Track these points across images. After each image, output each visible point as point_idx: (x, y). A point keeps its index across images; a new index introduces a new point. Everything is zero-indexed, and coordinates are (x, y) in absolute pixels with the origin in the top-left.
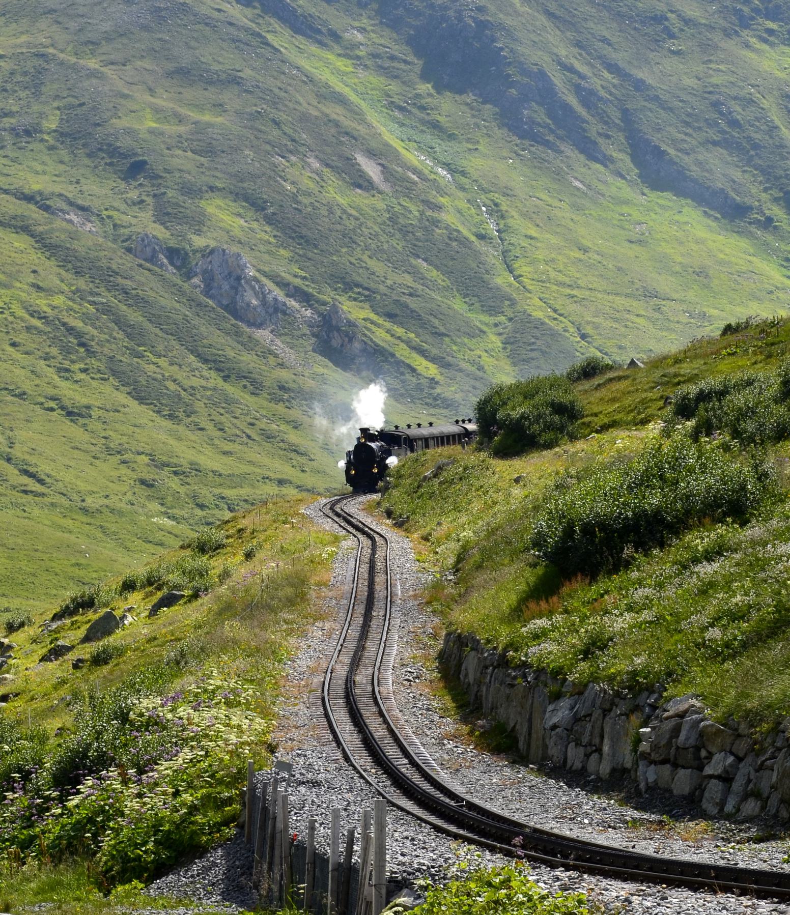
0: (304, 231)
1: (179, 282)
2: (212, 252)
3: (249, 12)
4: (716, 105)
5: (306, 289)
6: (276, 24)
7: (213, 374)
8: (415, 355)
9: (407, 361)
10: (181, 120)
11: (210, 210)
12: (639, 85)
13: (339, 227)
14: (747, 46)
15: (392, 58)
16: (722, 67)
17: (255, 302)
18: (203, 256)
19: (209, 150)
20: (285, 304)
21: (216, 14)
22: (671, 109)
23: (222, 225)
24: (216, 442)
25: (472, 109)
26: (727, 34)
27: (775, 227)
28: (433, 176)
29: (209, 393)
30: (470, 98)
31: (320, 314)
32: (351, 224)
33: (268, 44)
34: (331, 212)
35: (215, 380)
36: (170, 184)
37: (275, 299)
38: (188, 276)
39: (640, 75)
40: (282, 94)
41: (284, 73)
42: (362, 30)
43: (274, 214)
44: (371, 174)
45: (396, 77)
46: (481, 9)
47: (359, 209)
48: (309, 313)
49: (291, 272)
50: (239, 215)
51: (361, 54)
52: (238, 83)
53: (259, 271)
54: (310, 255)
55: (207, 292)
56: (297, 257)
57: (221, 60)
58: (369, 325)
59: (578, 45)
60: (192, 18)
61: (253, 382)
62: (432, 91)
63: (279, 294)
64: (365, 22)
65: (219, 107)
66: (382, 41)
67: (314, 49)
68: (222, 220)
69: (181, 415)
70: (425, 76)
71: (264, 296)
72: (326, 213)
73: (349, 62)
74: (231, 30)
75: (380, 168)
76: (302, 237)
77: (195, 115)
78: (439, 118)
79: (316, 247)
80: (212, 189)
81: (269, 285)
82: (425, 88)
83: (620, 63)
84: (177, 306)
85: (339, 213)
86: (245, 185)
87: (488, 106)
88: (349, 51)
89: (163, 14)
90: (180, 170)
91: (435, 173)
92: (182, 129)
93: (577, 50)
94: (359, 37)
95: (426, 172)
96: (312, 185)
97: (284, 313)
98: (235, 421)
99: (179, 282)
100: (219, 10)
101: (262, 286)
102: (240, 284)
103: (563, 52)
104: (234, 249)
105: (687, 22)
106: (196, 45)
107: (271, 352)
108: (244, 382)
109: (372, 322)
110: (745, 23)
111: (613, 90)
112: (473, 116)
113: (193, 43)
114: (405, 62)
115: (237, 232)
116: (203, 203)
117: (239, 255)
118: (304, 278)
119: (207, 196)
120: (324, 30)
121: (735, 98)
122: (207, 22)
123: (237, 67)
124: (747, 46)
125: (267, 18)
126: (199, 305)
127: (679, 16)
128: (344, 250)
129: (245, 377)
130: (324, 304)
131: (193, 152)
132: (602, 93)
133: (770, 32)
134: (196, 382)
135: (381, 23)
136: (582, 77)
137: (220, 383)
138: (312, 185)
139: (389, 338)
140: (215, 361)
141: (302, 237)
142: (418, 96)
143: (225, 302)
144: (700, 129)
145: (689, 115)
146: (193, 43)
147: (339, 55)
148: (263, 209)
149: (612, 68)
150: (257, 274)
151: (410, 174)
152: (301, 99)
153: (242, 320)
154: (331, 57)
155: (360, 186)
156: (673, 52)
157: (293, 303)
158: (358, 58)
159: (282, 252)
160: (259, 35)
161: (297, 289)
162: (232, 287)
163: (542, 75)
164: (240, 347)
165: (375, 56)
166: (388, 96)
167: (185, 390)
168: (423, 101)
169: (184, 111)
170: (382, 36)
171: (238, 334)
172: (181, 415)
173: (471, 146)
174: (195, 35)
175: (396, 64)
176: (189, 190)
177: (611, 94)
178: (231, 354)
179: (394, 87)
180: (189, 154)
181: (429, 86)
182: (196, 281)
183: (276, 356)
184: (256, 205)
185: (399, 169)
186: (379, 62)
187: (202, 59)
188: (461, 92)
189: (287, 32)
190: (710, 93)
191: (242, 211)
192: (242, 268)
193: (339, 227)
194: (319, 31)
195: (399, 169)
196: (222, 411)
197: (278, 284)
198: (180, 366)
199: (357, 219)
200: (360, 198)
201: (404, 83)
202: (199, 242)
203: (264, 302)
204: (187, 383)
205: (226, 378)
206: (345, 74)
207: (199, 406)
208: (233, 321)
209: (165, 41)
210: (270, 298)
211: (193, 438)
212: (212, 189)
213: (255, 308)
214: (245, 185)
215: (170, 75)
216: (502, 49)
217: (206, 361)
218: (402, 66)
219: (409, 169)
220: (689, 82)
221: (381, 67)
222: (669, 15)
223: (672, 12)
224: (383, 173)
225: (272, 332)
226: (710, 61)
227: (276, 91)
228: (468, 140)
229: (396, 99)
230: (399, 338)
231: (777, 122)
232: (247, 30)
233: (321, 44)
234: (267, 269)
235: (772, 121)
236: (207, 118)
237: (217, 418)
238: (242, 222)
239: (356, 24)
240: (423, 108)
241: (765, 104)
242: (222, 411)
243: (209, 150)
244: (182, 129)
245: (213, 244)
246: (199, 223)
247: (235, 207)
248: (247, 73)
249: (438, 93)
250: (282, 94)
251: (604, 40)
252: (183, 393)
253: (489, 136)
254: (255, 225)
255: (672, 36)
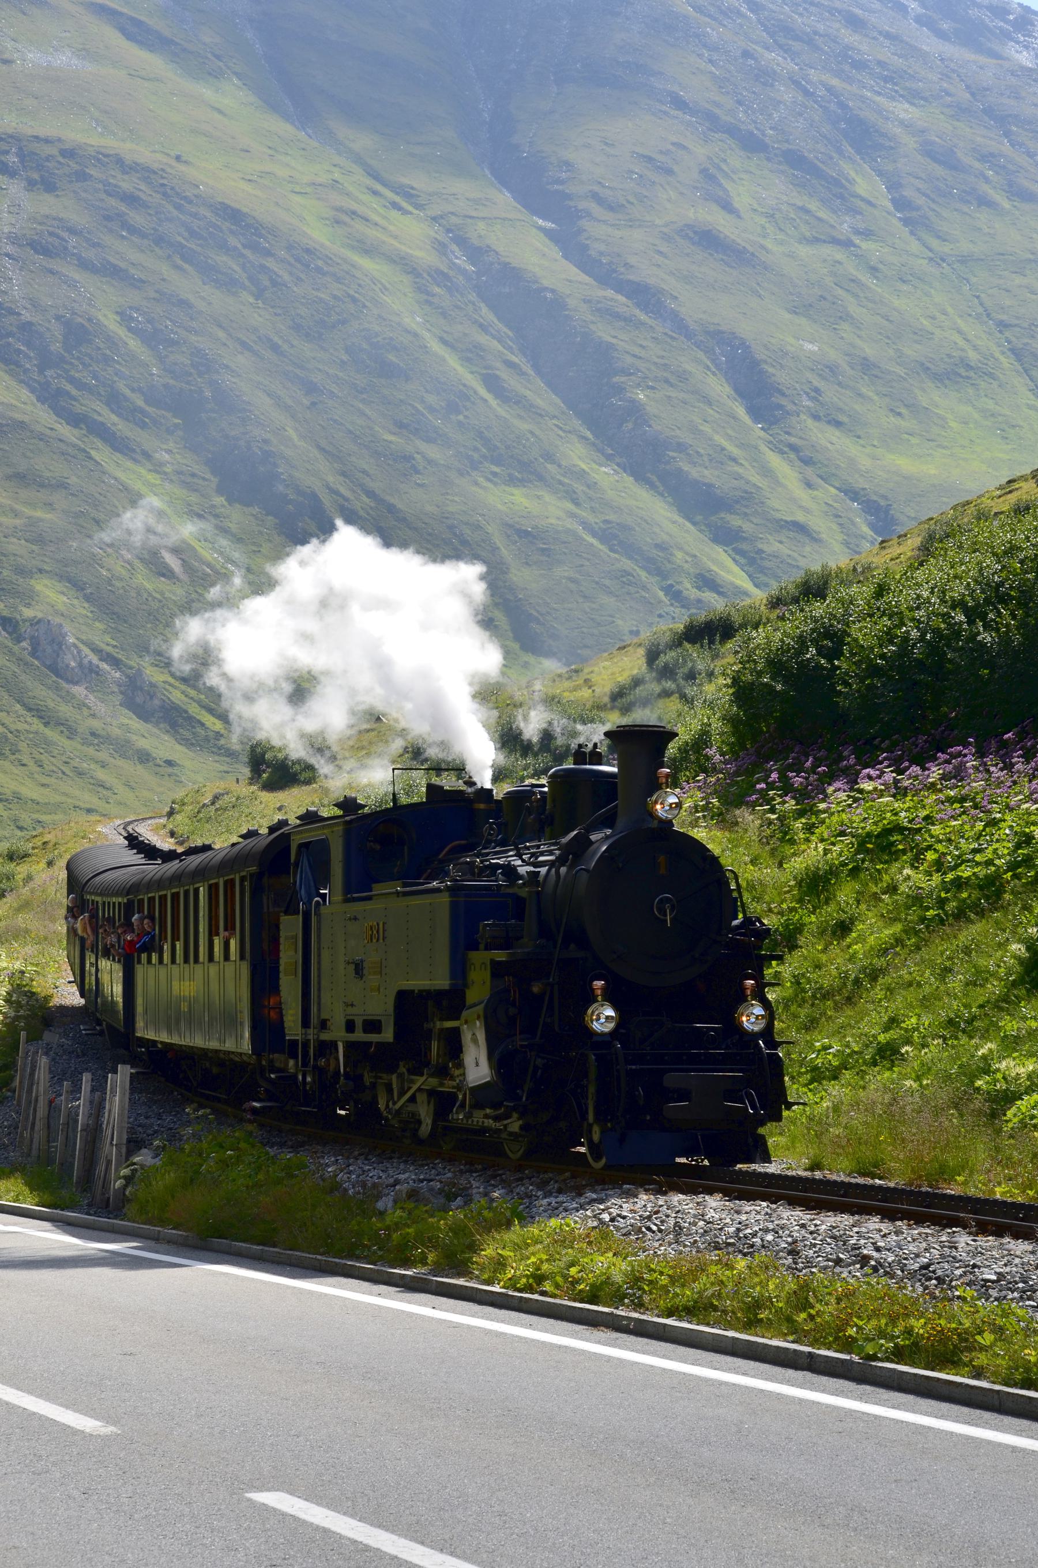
0: (116, 609)
1: (10, 644)
2: (39, 621)
3: (76, 431)
4: (451, 527)
5: (115, 655)
6: (99, 444)
7: (35, 720)
8: (204, 712)
9: (198, 717)
10: (16, 514)
11: (39, 587)
12: (391, 509)
13: (145, 607)
14: (476, 483)
15: (193, 475)
16: (456, 499)
17: (73, 664)
18: (31, 625)
19: (39, 540)
20: (98, 667)
21: (48, 432)
22: (416, 529)
23: (48, 600)
24: (36, 776)
25: (257, 519)
26: (461, 473)
27: (496, 626)
28: (224, 571)
29: (31, 736)
30: (256, 510)
31: (127, 676)
32: (155, 605)
33: (91, 458)
34: (139, 594)
35: (37, 725)
36: (5, 565)
37: (90, 662)
38: (19, 640)
39: (392, 501)
40: (102, 498)
41: (104, 482)
42: (169, 451)
43: (91, 594)
44: (173, 566)
45: (196, 490)
46: (265, 441)
47: (162, 594)
48: (118, 675)
49: (105, 641)
50: (63, 593)
51: (167, 470)
52: (66, 488)
53: (77, 639)
54: (121, 628)
55: (33, 654)
56: (110, 629)
57: (51, 468)
58: (167, 687)
59: (344, 474)
60: (29, 434)
61: (70, 728)
62: (225, 503)
63: (95, 660)
64: (171, 445)
65: (49, 506)
66: (185, 461)
67: (129, 464)
68: (48, 596)
69: (7, 753)
70: (220, 491)
71: (81, 659)
72: (135, 595)
73: (158, 476)
74: (61, 445)
75: (180, 562)
76: (114, 614)
77: (27, 511)
78: (230, 525)
79: (125, 622)
80: (41, 571)
81: (86, 650)
82: (220, 500)
83: (377, 492)
84: (8, 664)
85: (145, 595)
86: (69, 569)
87: (270, 518)
88: (157, 468)
89: (5, 429)
90: (15, 555)
91: (226, 568)
92: (18, 522)
93: (341, 478)
94: (167, 457)
95: (218, 567)
96: (124, 572)
97: (97, 674)
98: (52, 759)
99: (10, 644)
100: (52, 429)
101: (79, 652)
102: (60, 648)
103: (330, 479)
104: (58, 620)
105: (430, 462)
106: (32, 455)
107: (85, 705)
108: (62, 728)
109: (170, 685)
110: (474, 466)
111: (371, 512)
112: (258, 525)
113: (29, 454)
114: (204, 479)
115: (61, 607)
116: (33, 582)
117: (61, 625)
118: (115, 647)
119: (36, 576)
120: (138, 450)
121: (467, 524)
122: (41, 437)
123: (65, 475)
124: (476, 483)
125: (91, 437)
126: (26, 664)
127: (424, 457)
128: (149, 626)
129: (62, 724)
130: (131, 668)
131: (26, 540)
132: (362, 513)
133: (495, 474)
134: (21, 726)
135: (185, 447)
136: (347, 500)
137: (41, 727)
138: (124, 572)
139: (183, 697)
140: (38, 710)
141: (114, 614)
142: (213, 506)
143: (48, 663)
144: (438, 545)
145: (430, 534)
146: (29, 454)
147: (150, 470)
148: (83, 589)
149: (370, 494)
150: (76, 642)
151: (205, 568)
152: (117, 503)
153: (61, 678)
154: (143, 472)
155: (163, 575)
156: (419, 485)
157: (105, 666)
158: (165, 473)
159: (97, 624)
160: (84, 451)
161: (109, 655)
162: (54, 651)
163: (314, 496)
164: (59, 700)
165: (180, 473)
166: (190, 505)
167: (11, 733)
168: (217, 511)
169: (18, 507)
170: (186, 458)
171: (58, 689)
172: (7, 753)
173: (256, 549)
174: (31, 447)
175: (195, 480)
176: (21, 571)
177: (368, 514)
178: (51, 704)
179: (194, 498)
180: (23, 542)
181: (223, 499)
182: (24, 644)
183: (89, 708)
184: (77, 585)
185: (196, 564)
186: (183, 478)
187: (36, 467)
188: (248, 505)
189: (107, 450)
190: (447, 518)
191: (65, 590)
192: (64, 636)
193: (145, 607)
194: (134, 451)
195: (196, 564)
196: (42, 751)
197: (93, 650)
198: (8, 712)
199: (160, 601)
200: (163, 584)
201: (202, 495)
202: (28, 613)
203: (81, 665)
204: (13, 727)
205: (46, 724)
206: (155, 485)
207: (23, 746)
208: (54, 678)
209: (6, 451)
210: (86, 661)
211: (16, 772)
212: (41, 571)
213: (73, 669)
214: (69, 569)
215: (9, 478)
216: (282, 474)
217: (30, 710)
218: (201, 482)
219: (204, 563)
220: (429, 508)
221: (184, 482)
222: (416, 455)
223: (418, 453)
224: (183, 566)
225: (86, 688)
226: (447, 493)
227: (97, 496)
228: (254, 544)
229: (195, 508)
230: (192, 698)
231: (499, 545)
232: (74, 446)
233: (135, 460)
234: (84, 638)
235: (495, 543)
236: (39, 514)
237: (38, 756)
238: (65, 599)
239: (165, 447)
240: (216, 516)
241: (490, 529)
242: (42, 751)
243: (39, 540)
244: (18, 522)
245: (40, 615)
246: (29, 597)
247: (59, 586)
248: (73, 480)
249: (230, 505)
250: (102, 498)
251: (364, 472)
252: (9, 735)
253: (270, 541)
254: (76, 602)
255: (417, 472)
